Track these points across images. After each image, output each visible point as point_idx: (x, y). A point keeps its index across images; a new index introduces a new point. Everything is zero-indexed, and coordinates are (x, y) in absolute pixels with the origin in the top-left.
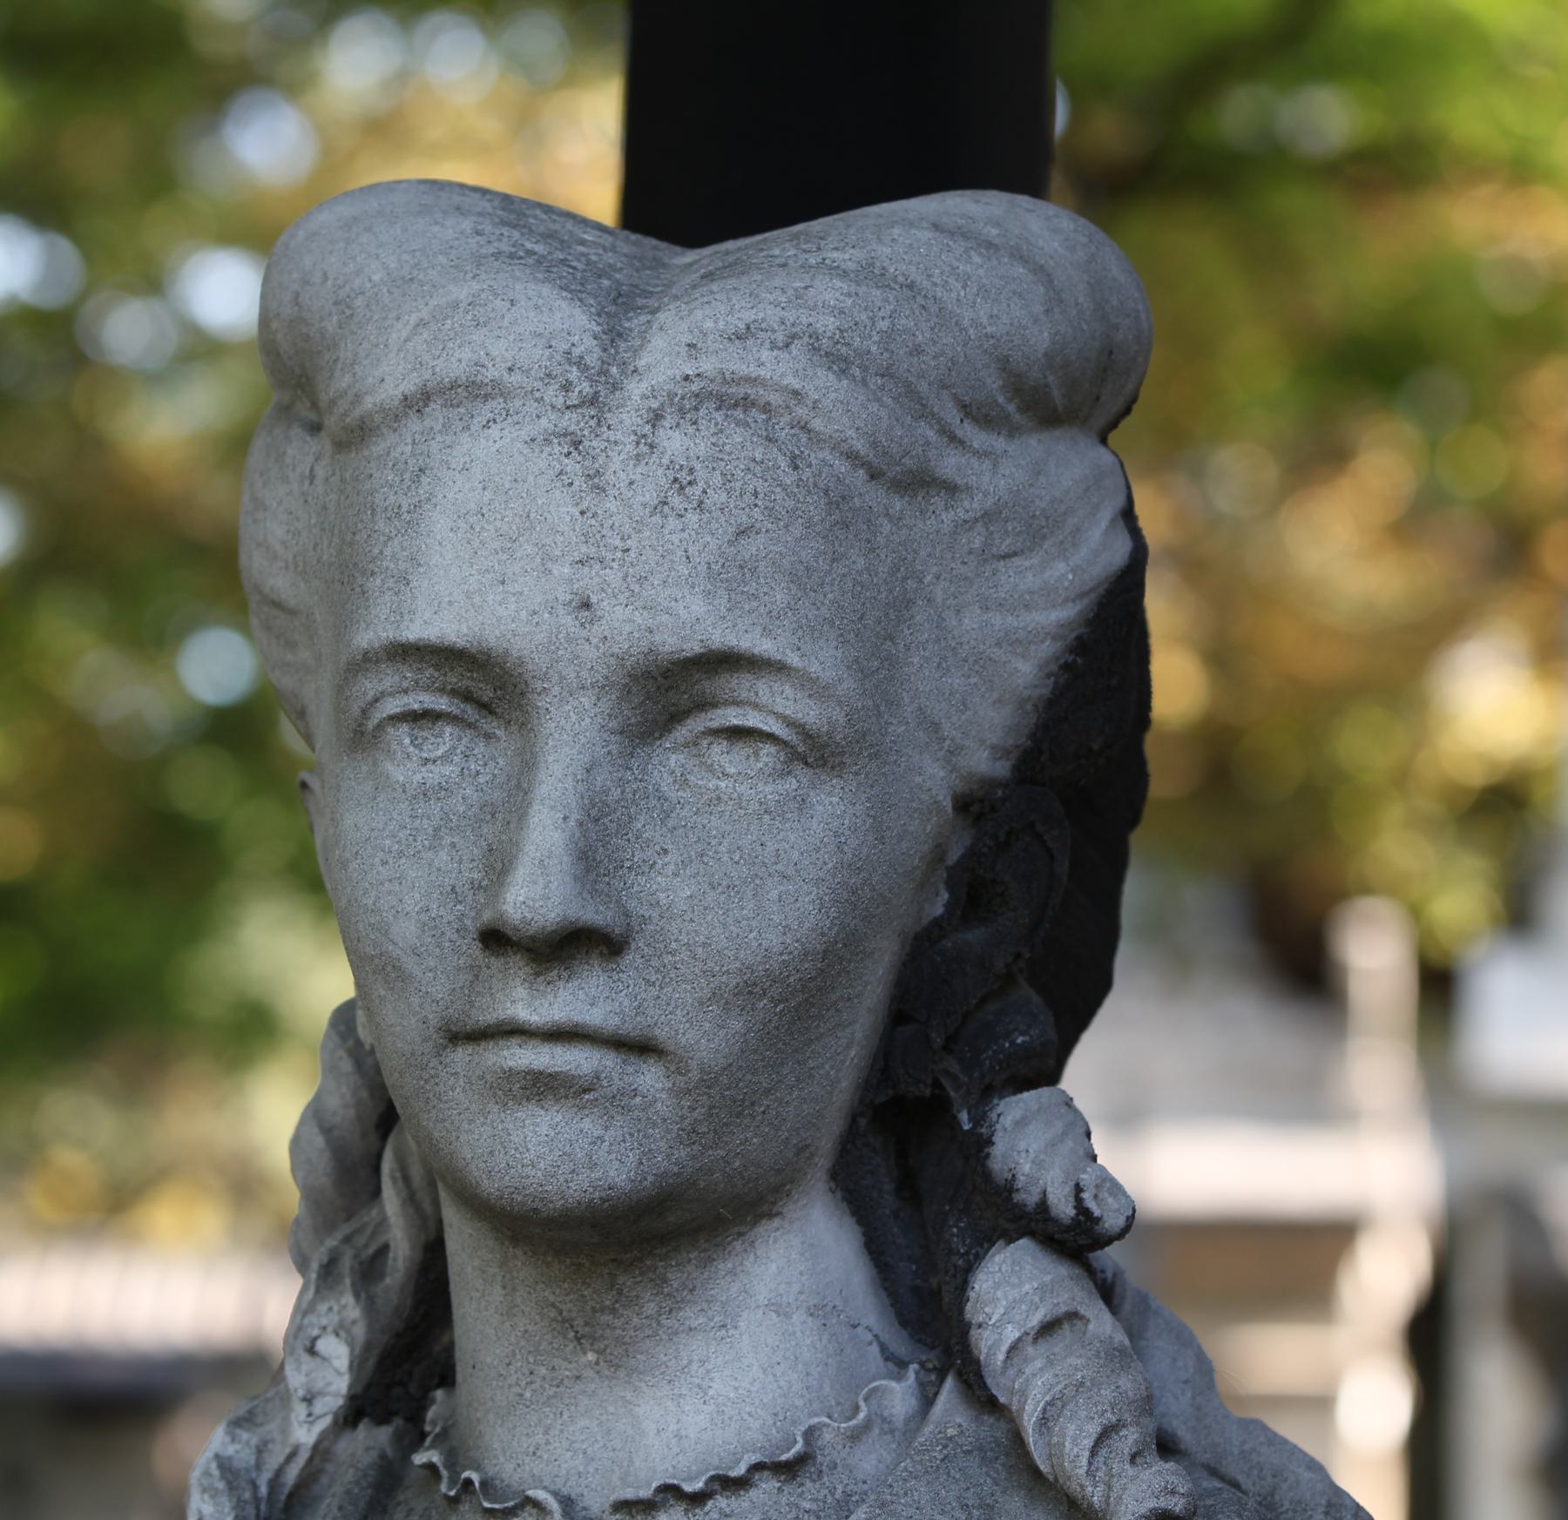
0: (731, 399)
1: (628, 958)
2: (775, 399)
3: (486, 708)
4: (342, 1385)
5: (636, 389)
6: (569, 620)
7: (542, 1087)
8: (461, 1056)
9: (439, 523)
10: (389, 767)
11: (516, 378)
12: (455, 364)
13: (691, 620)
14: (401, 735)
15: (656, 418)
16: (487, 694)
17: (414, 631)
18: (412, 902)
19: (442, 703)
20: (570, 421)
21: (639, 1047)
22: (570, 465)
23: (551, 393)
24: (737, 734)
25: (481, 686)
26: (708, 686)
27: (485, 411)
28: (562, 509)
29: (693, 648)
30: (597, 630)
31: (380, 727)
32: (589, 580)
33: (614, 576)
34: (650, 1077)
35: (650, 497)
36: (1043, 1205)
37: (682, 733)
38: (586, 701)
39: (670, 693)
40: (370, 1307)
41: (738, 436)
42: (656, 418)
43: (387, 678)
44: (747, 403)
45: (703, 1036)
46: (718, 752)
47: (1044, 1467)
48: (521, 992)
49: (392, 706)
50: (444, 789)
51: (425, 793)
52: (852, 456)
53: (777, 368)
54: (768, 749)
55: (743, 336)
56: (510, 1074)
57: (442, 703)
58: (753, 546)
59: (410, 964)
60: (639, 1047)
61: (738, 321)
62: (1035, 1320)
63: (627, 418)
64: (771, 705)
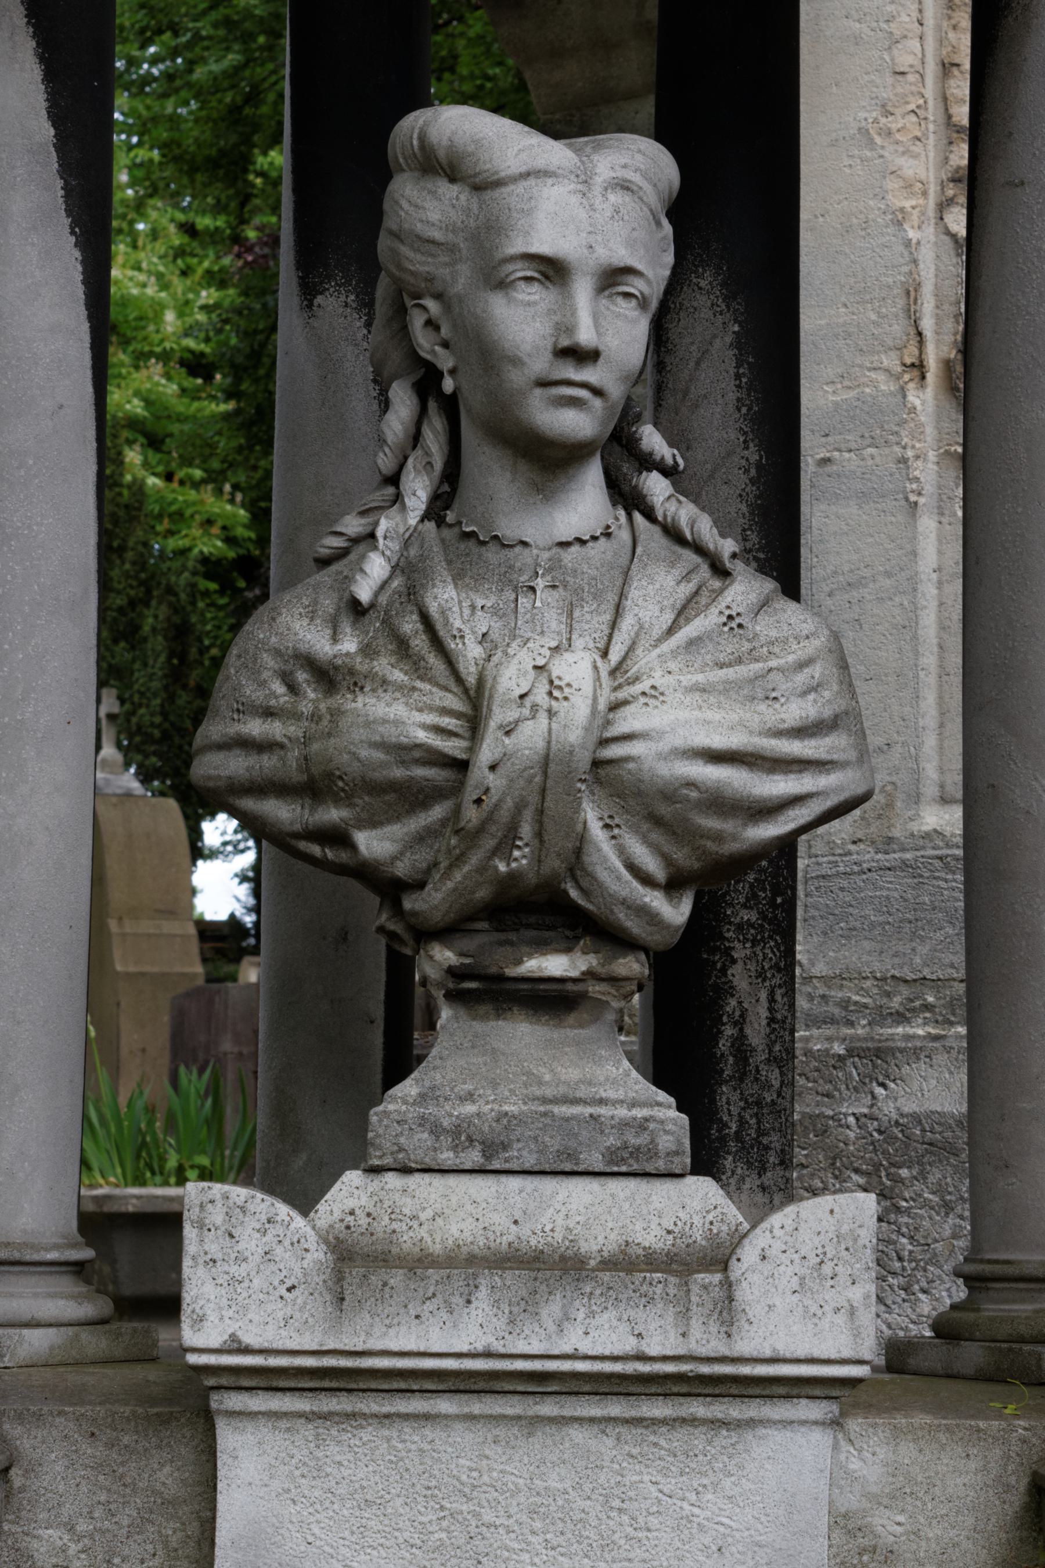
0: (625, 186)
1: (601, 360)
2: (635, 188)
3: (547, 277)
4: (424, 507)
5: (599, 180)
6: (585, 251)
7: (574, 402)
8: (538, 392)
9: (541, 215)
10: (515, 294)
11: (560, 171)
12: (540, 163)
13: (623, 256)
14: (522, 284)
15: (606, 189)
16: (551, 273)
17: (533, 250)
18: (529, 338)
19: (536, 275)
20: (580, 187)
21: (597, 392)
22: (584, 201)
23: (572, 177)
24: (627, 295)
25: (552, 270)
26: (619, 279)
27: (550, 181)
28: (583, 215)
29: (622, 265)
30: (595, 255)
31: (514, 281)
32: (591, 239)
33: (599, 239)
34: (597, 403)
35: (609, 214)
36: (663, 458)
37: (607, 293)
38: (589, 278)
39: (612, 278)
40: (431, 480)
41: (627, 199)
42: (606, 189)
43: (519, 265)
44: (628, 189)
45: (616, 391)
46: (620, 300)
47: (689, 537)
48: (571, 370)
49: (520, 274)
50: (535, 303)
51: (529, 304)
52: (651, 210)
53: (636, 178)
54: (634, 302)
55: (625, 166)
56: (563, 397)
57: (536, 275)
58: (635, 234)
59: (526, 359)
60: (597, 392)
61: (623, 161)
62: (667, 495)
63: (597, 190)
64: (636, 286)
